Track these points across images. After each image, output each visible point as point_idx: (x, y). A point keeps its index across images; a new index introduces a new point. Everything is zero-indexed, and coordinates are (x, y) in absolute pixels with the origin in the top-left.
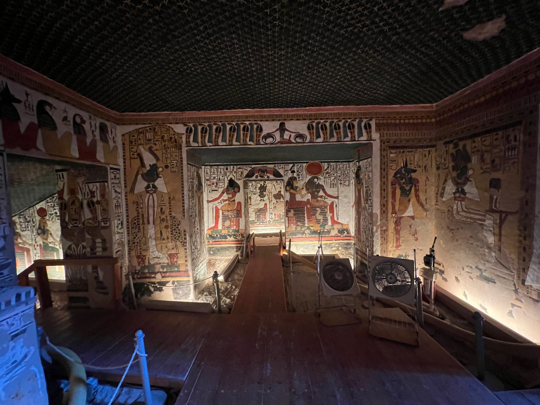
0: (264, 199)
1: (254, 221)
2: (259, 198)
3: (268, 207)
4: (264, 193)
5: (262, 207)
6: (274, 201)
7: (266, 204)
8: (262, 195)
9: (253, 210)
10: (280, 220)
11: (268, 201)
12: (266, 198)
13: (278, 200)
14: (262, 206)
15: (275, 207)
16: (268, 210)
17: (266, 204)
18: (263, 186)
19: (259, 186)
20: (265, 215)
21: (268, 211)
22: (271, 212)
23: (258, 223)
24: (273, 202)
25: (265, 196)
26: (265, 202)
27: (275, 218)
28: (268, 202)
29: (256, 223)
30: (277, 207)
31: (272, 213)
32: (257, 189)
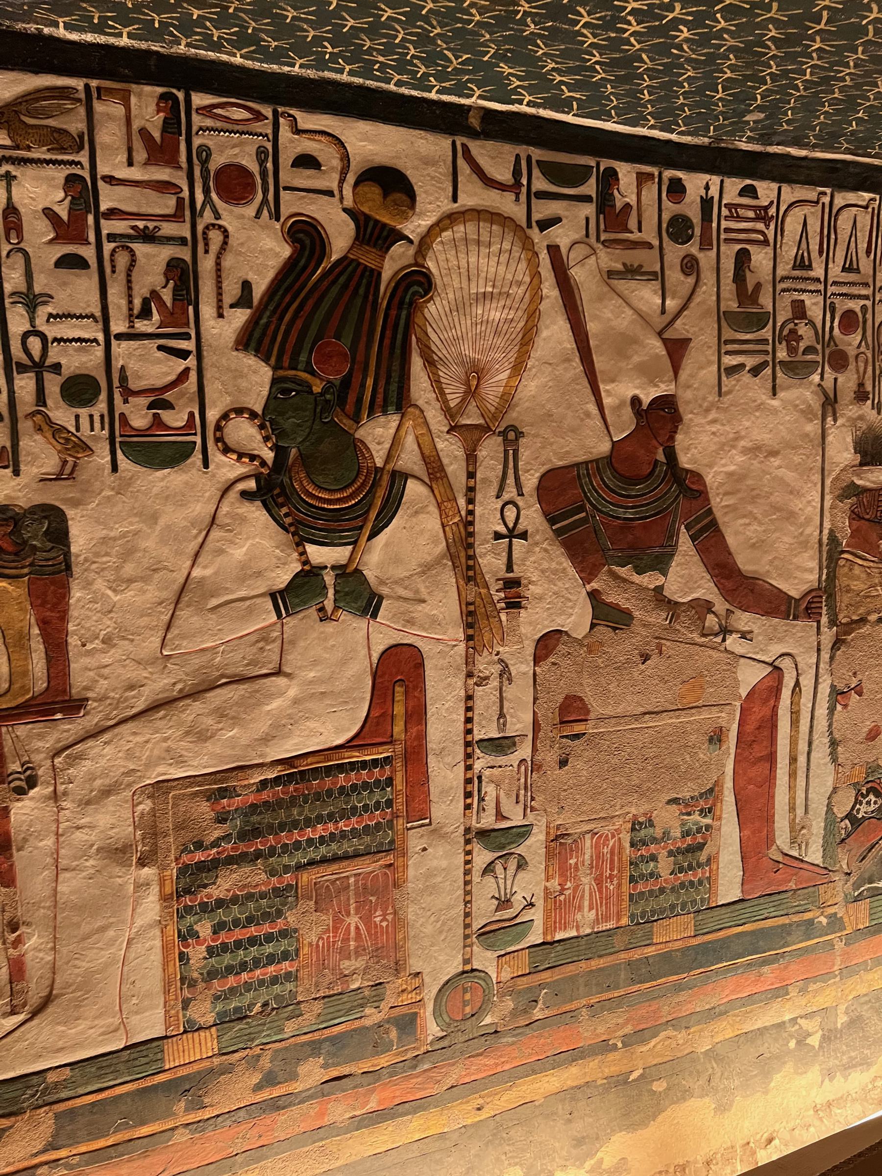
0: (377, 558)
1: (143, 1052)
2: (259, 547)
3: (443, 724)
4: (377, 434)
5: (329, 728)
6: (557, 597)
7: (398, 674)
8: (319, 483)
9: (115, 820)
10: (645, 921)
11: (444, 603)
12: (405, 544)
13: (628, 585)
14: (314, 706)
15: (572, 710)
16: (445, 774)
17: (398, 674)
18: (356, 276)
19: (258, 251)
20: (386, 890)
21: (447, 808)
22: (502, 803)
23: (238, 1090)
24: (533, 622)
25: (375, 500)
26: (382, 633)
27: (559, 906)
28: (432, 622)
29: (192, 1087)
30: (612, 700)
31: (501, 839)
32: (221, 328)
